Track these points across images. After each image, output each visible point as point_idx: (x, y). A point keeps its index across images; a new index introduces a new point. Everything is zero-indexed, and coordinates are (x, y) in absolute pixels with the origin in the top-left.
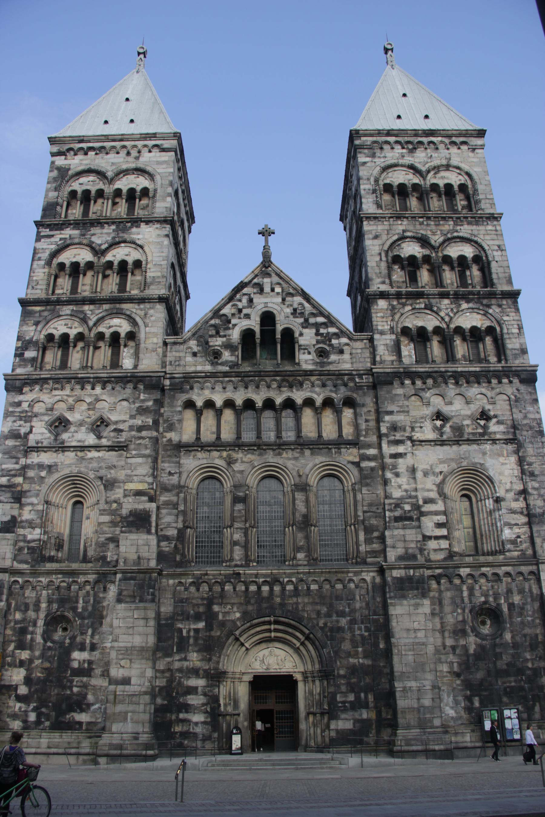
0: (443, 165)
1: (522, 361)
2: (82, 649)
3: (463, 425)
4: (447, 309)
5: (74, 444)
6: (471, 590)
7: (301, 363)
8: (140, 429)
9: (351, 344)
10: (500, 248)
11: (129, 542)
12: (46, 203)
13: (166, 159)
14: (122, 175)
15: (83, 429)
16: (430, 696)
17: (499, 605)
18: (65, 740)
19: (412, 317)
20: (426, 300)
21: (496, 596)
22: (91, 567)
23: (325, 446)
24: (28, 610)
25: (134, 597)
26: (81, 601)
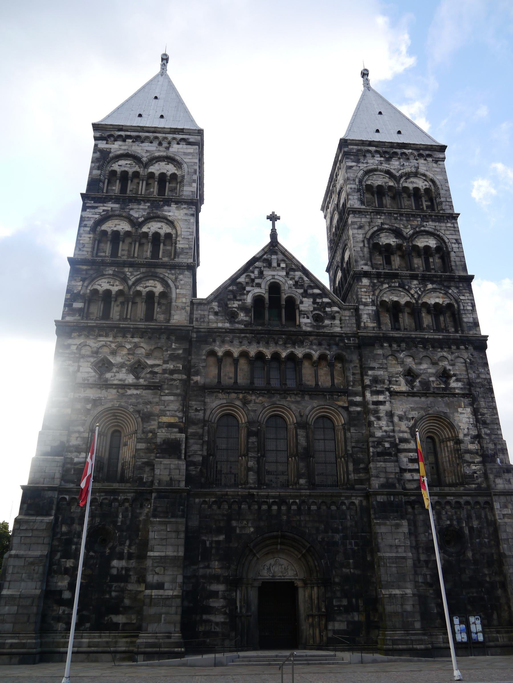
0: (412, 172)
1: (475, 332)
2: (120, 557)
3: (429, 381)
4: (416, 288)
5: (116, 382)
8: (172, 372)
9: (341, 312)
10: (458, 242)
11: (162, 467)
12: (90, 179)
13: (191, 151)
14: (154, 161)
15: (124, 370)
16: (411, 602)
17: (461, 528)
18: (104, 640)
19: (389, 293)
20: (400, 280)
21: (459, 520)
22: (130, 487)
24: (74, 523)
26: (120, 516)
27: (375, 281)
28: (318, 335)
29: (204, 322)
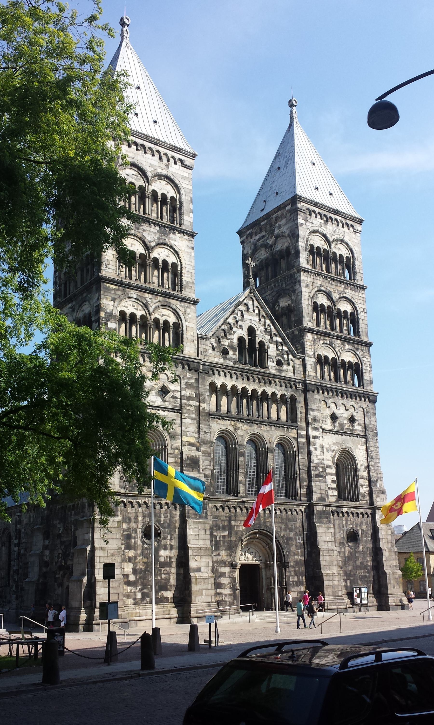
1: (370, 388)
2: (165, 549)
6: (346, 520)
8: (189, 398)
23: (282, 426)
26: (163, 517)
27: (316, 337)
28: (282, 378)
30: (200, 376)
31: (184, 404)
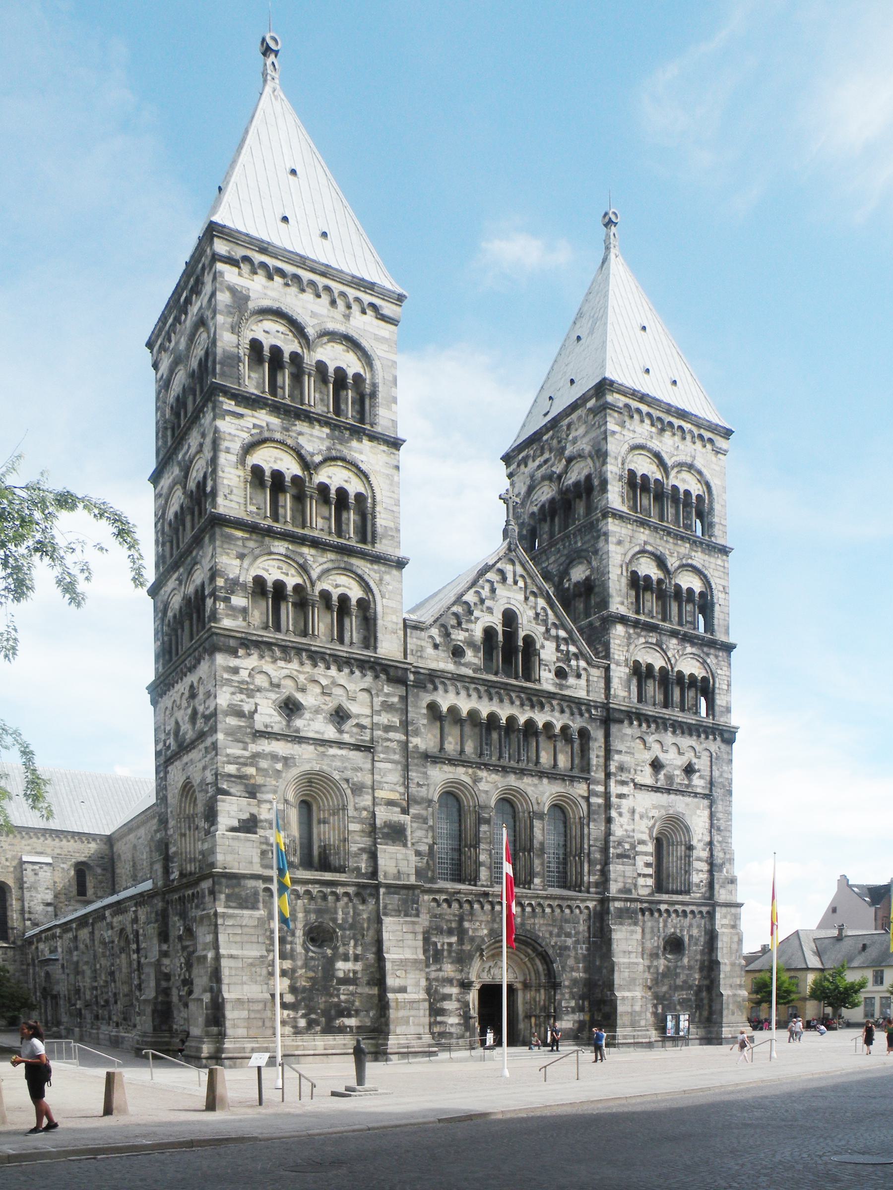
6: (665, 922)
7: (542, 681)
8: (388, 728)
10: (725, 590)
17: (683, 935)
25: (399, 911)
29: (421, 657)
30: (410, 692)
31: (379, 738)
